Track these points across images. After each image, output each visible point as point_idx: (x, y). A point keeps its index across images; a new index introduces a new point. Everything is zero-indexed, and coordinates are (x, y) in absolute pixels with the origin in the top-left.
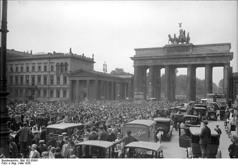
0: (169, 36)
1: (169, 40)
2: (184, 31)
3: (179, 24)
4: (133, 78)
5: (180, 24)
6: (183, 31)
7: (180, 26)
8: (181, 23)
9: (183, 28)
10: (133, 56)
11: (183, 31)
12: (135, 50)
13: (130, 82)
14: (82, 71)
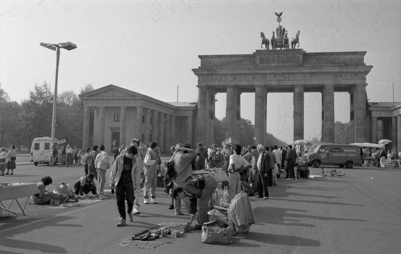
0: (262, 35)
1: (263, 41)
2: (284, 28)
3: (276, 14)
4: (196, 106)
5: (279, 16)
6: (282, 28)
7: (279, 20)
8: (281, 14)
9: (283, 24)
10: (198, 68)
11: (282, 28)
12: (200, 57)
13: (190, 114)
14: (112, 89)
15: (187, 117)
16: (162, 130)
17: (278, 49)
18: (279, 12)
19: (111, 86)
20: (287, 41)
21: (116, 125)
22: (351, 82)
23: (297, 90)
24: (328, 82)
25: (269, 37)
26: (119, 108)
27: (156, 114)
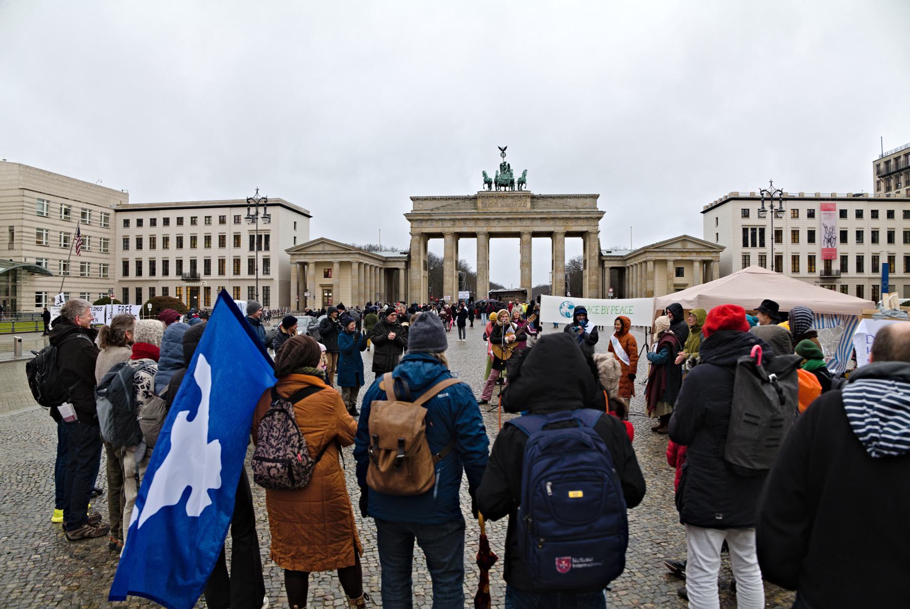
0: (484, 174)
5: (503, 150)
7: (503, 154)
9: (507, 160)
12: (412, 199)
13: (401, 266)
15: (398, 269)
16: (373, 286)
17: (503, 188)
18: (503, 147)
19: (322, 239)
20: (512, 182)
21: (327, 281)
22: (584, 229)
23: (526, 237)
24: (559, 228)
25: (492, 176)
26: (331, 263)
27: (368, 268)
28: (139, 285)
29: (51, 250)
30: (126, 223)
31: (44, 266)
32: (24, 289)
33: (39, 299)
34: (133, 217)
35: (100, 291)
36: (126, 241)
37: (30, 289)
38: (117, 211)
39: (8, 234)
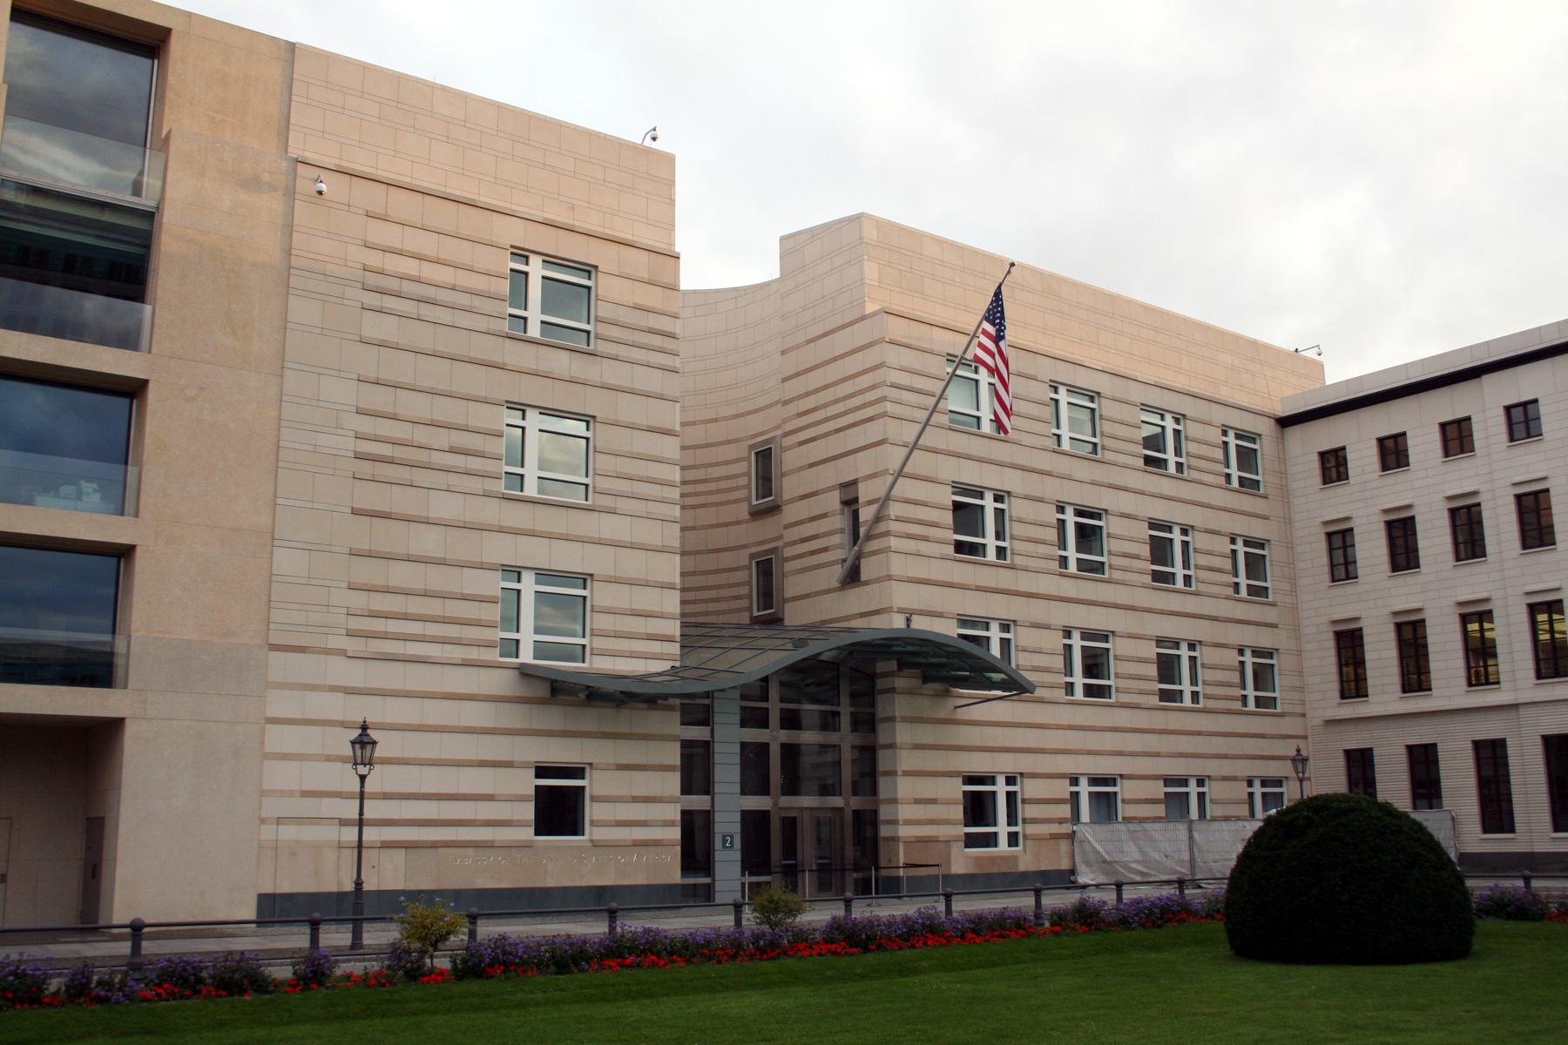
28: (1420, 735)
29: (1024, 582)
30: (1334, 466)
31: (995, 650)
32: (907, 760)
33: (978, 808)
34: (1359, 437)
35: (1245, 768)
36: (1340, 541)
37: (933, 761)
38: (1285, 422)
39: (839, 521)
